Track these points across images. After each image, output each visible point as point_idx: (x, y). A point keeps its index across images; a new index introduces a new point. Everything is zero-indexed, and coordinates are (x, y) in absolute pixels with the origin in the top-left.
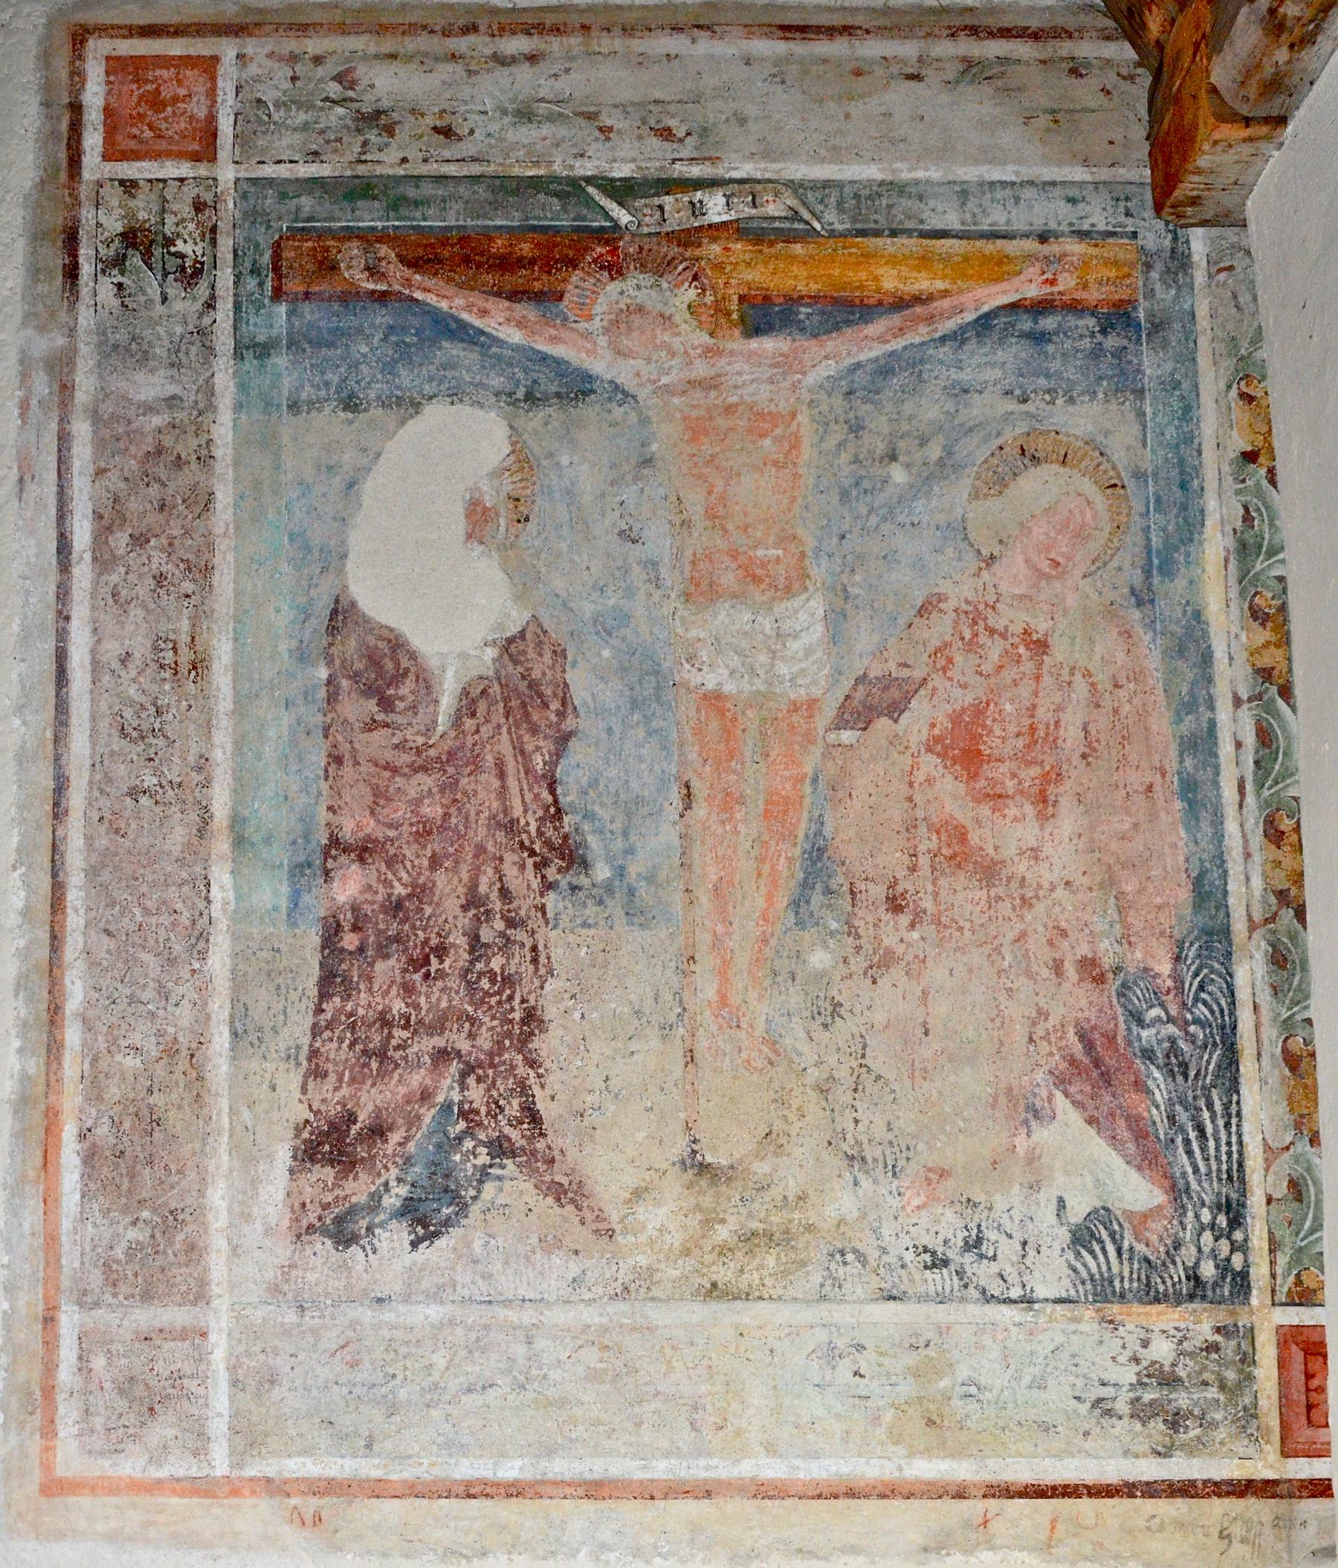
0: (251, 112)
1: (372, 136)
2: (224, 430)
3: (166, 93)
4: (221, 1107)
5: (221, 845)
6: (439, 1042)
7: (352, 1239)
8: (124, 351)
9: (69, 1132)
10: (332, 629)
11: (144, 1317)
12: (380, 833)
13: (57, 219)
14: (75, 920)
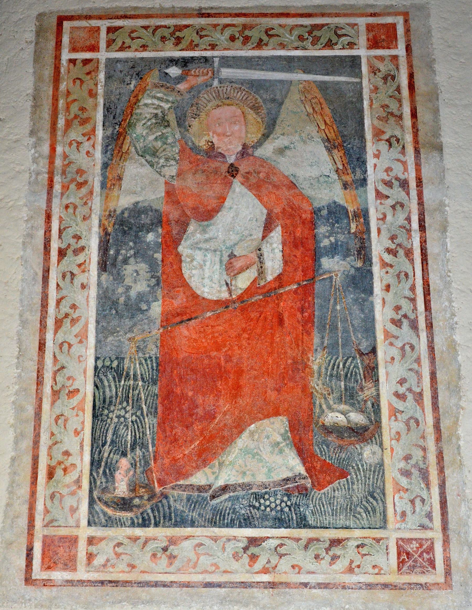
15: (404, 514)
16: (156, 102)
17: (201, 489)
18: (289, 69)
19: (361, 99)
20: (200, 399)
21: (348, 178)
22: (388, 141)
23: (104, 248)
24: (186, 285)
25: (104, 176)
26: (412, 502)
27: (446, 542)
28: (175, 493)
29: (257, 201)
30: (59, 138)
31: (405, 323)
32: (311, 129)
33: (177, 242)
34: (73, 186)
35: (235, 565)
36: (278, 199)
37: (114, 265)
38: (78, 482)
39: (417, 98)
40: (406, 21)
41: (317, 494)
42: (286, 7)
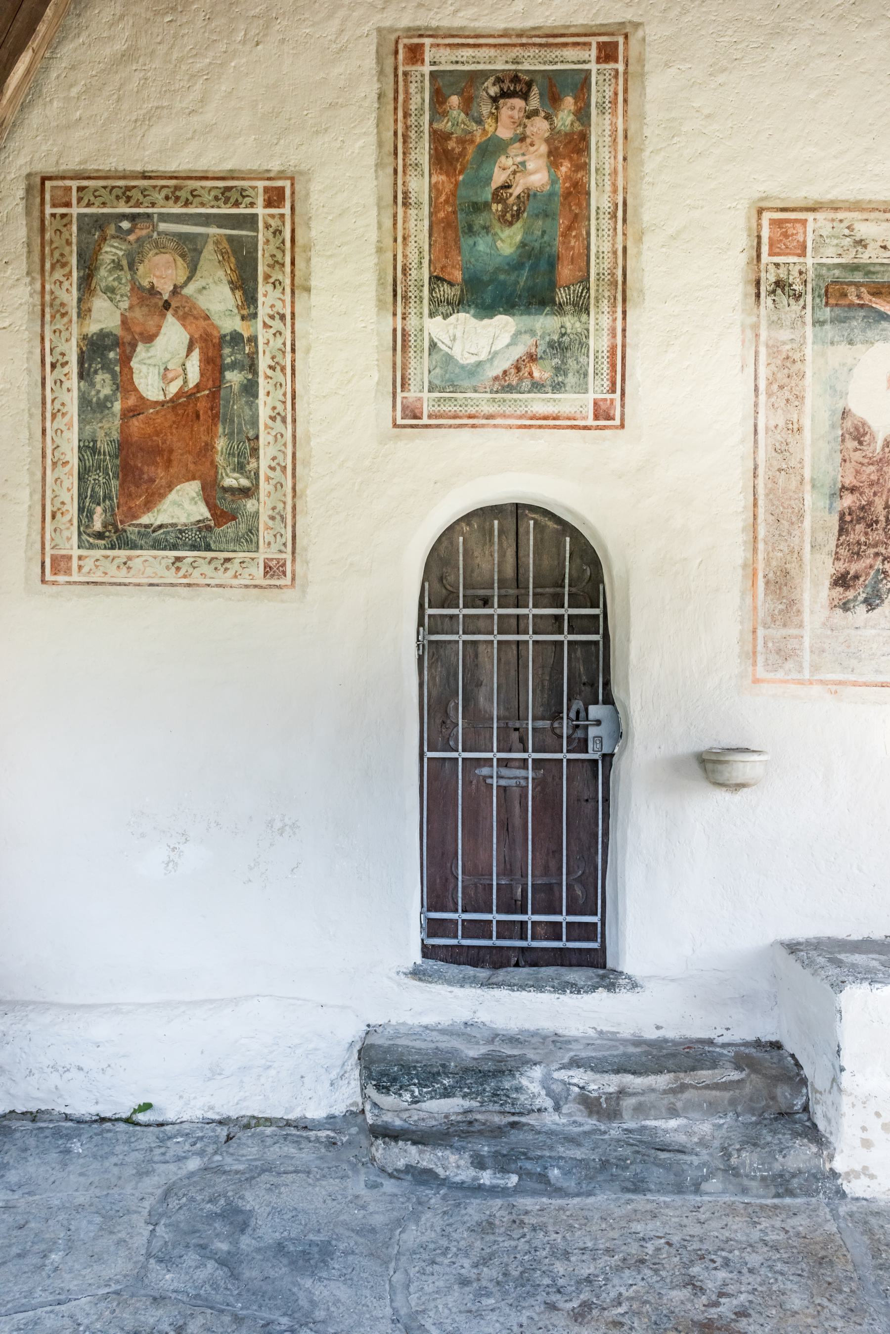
0: (818, 239)
1: (859, 248)
2: (808, 350)
3: (789, 232)
4: (807, 568)
5: (808, 487)
6: (876, 550)
7: (848, 610)
8: (775, 323)
9: (760, 575)
10: (843, 418)
11: (784, 632)
12: (858, 484)
13: (753, 277)
14: (761, 511)
15: (269, 544)
16: (114, 250)
17: (147, 526)
18: (207, 225)
19: (256, 250)
20: (146, 469)
21: (245, 312)
22: (274, 283)
23: (81, 362)
24: (136, 390)
25: (79, 307)
26: (275, 536)
27: (294, 560)
28: (131, 529)
29: (182, 329)
30: (47, 278)
31: (278, 418)
32: (221, 273)
33: (129, 359)
34: (58, 316)
35: (167, 573)
36: (197, 327)
37: (88, 375)
38: (71, 521)
39: (297, 249)
40: (292, 184)
41: (217, 530)
42: (206, 171)
